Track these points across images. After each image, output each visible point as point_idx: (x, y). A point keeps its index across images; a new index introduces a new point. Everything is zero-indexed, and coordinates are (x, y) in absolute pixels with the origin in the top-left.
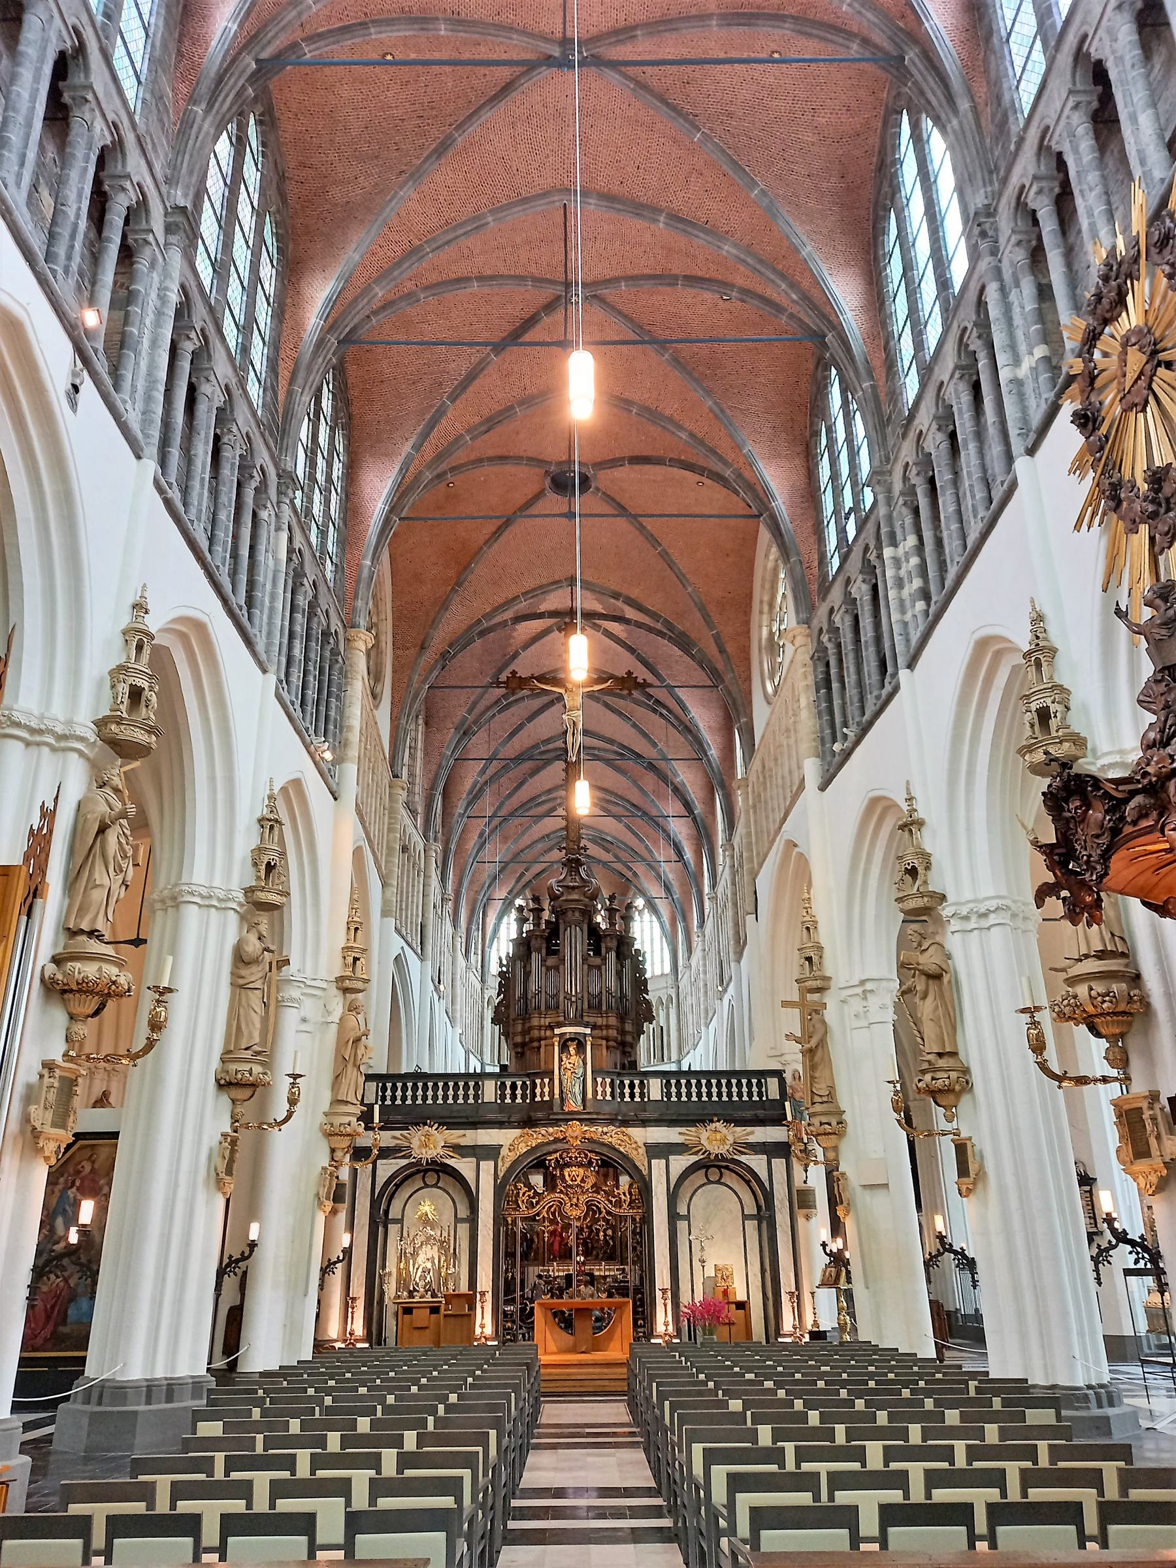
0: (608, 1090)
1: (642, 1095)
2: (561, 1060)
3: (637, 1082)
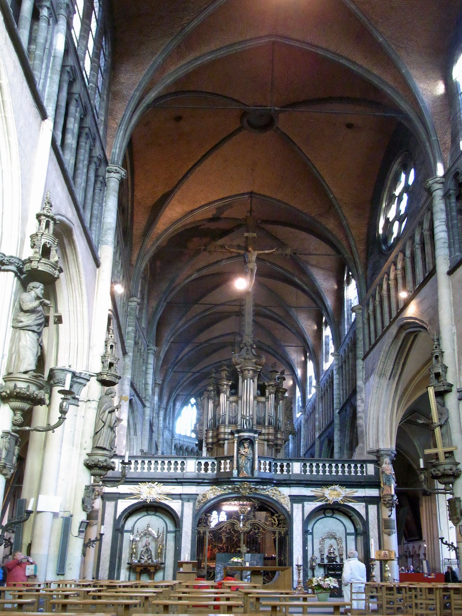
0: (268, 467)
3: (285, 464)
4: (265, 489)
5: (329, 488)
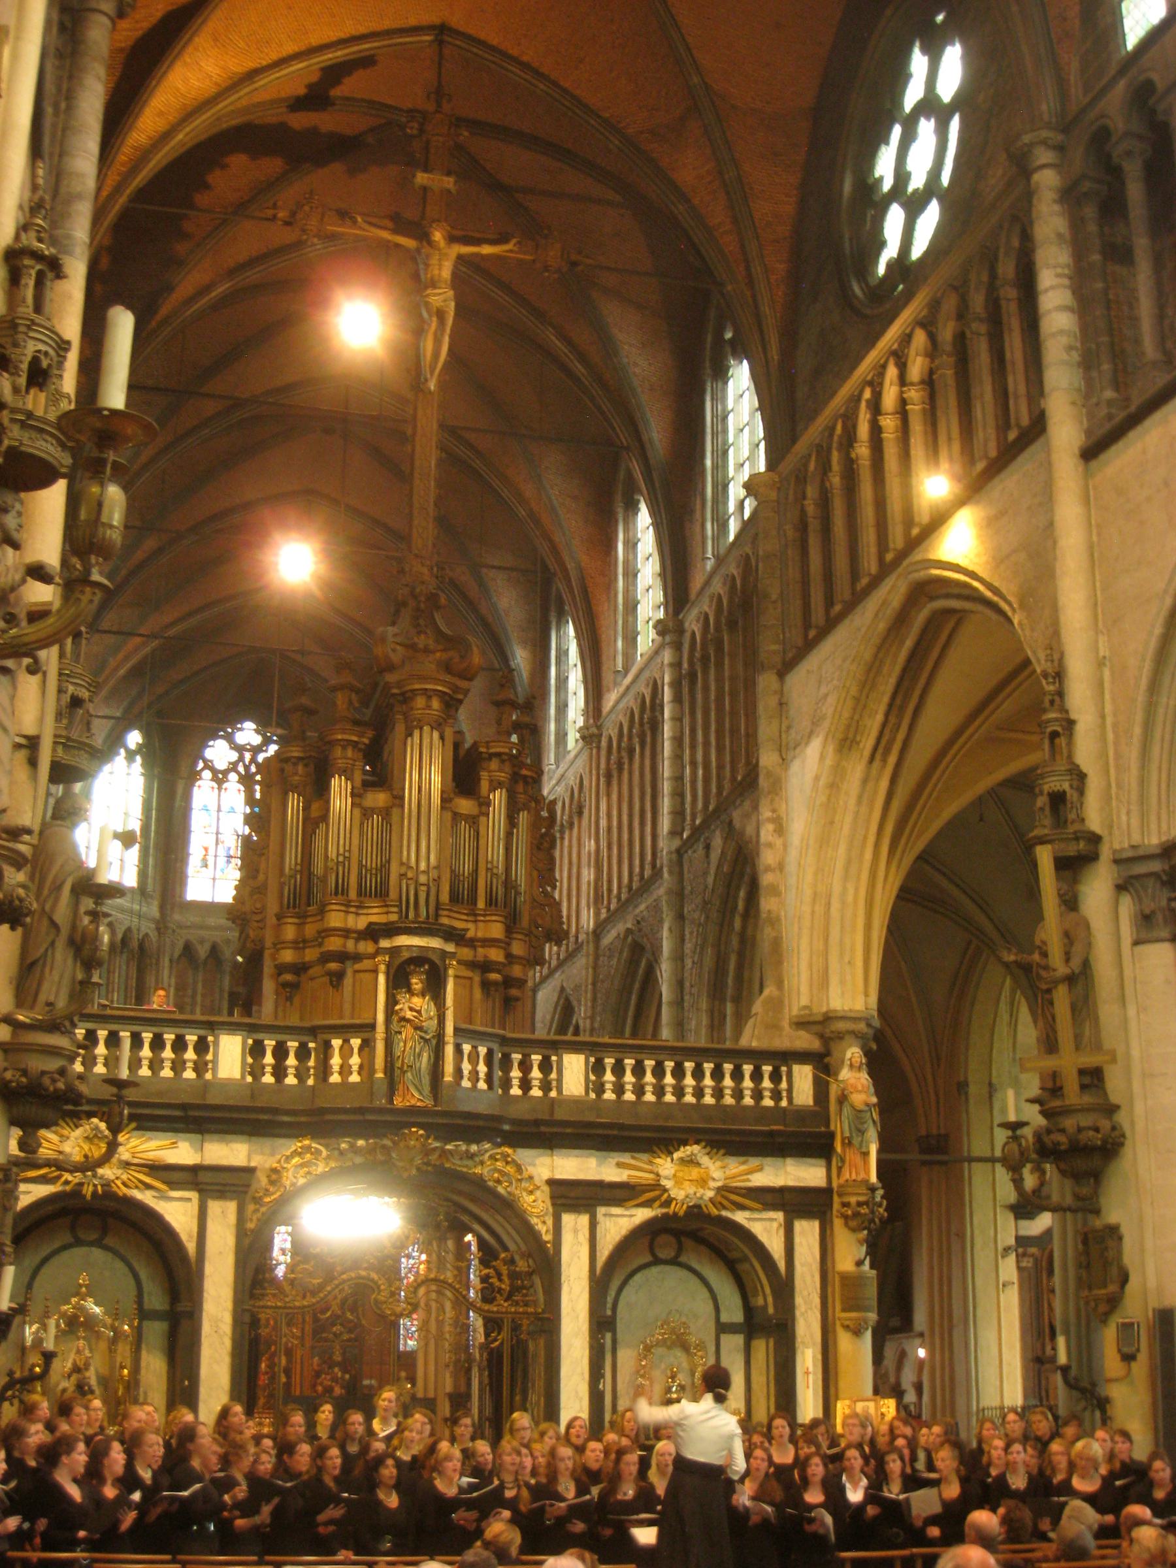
0: (482, 1069)
1: (546, 1086)
2: (391, 1002)
4: (472, 1156)
5: (676, 1155)
